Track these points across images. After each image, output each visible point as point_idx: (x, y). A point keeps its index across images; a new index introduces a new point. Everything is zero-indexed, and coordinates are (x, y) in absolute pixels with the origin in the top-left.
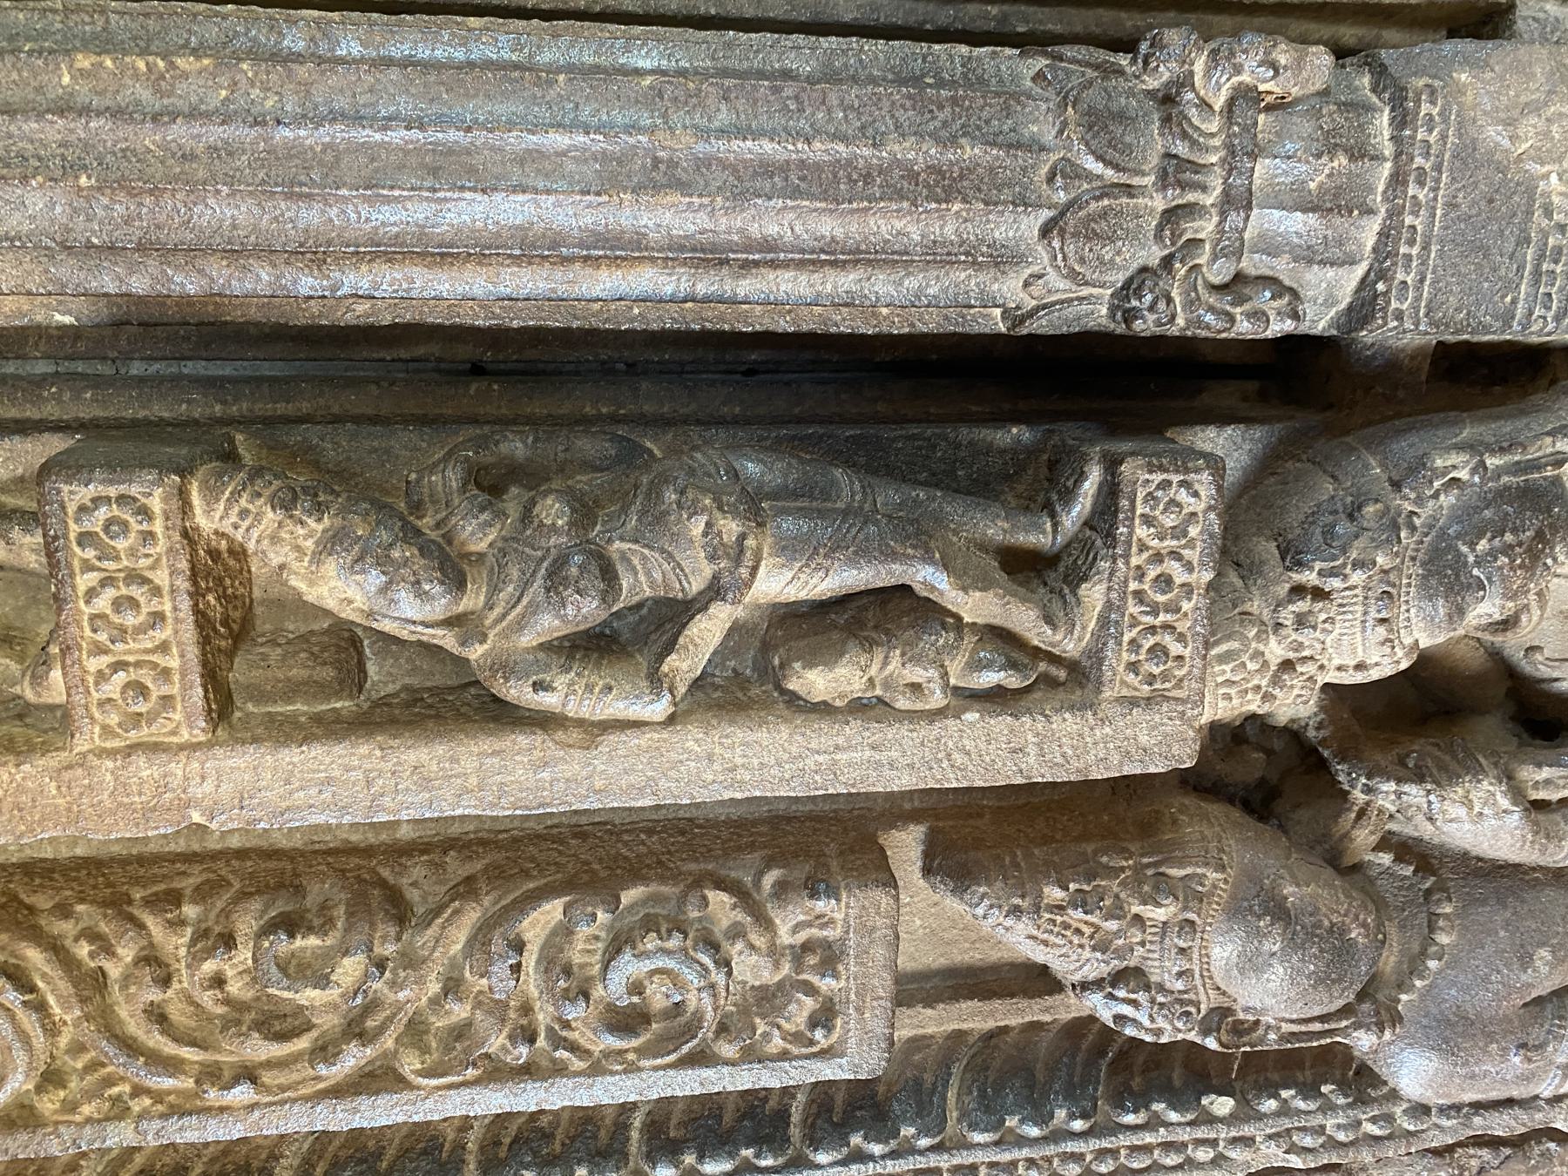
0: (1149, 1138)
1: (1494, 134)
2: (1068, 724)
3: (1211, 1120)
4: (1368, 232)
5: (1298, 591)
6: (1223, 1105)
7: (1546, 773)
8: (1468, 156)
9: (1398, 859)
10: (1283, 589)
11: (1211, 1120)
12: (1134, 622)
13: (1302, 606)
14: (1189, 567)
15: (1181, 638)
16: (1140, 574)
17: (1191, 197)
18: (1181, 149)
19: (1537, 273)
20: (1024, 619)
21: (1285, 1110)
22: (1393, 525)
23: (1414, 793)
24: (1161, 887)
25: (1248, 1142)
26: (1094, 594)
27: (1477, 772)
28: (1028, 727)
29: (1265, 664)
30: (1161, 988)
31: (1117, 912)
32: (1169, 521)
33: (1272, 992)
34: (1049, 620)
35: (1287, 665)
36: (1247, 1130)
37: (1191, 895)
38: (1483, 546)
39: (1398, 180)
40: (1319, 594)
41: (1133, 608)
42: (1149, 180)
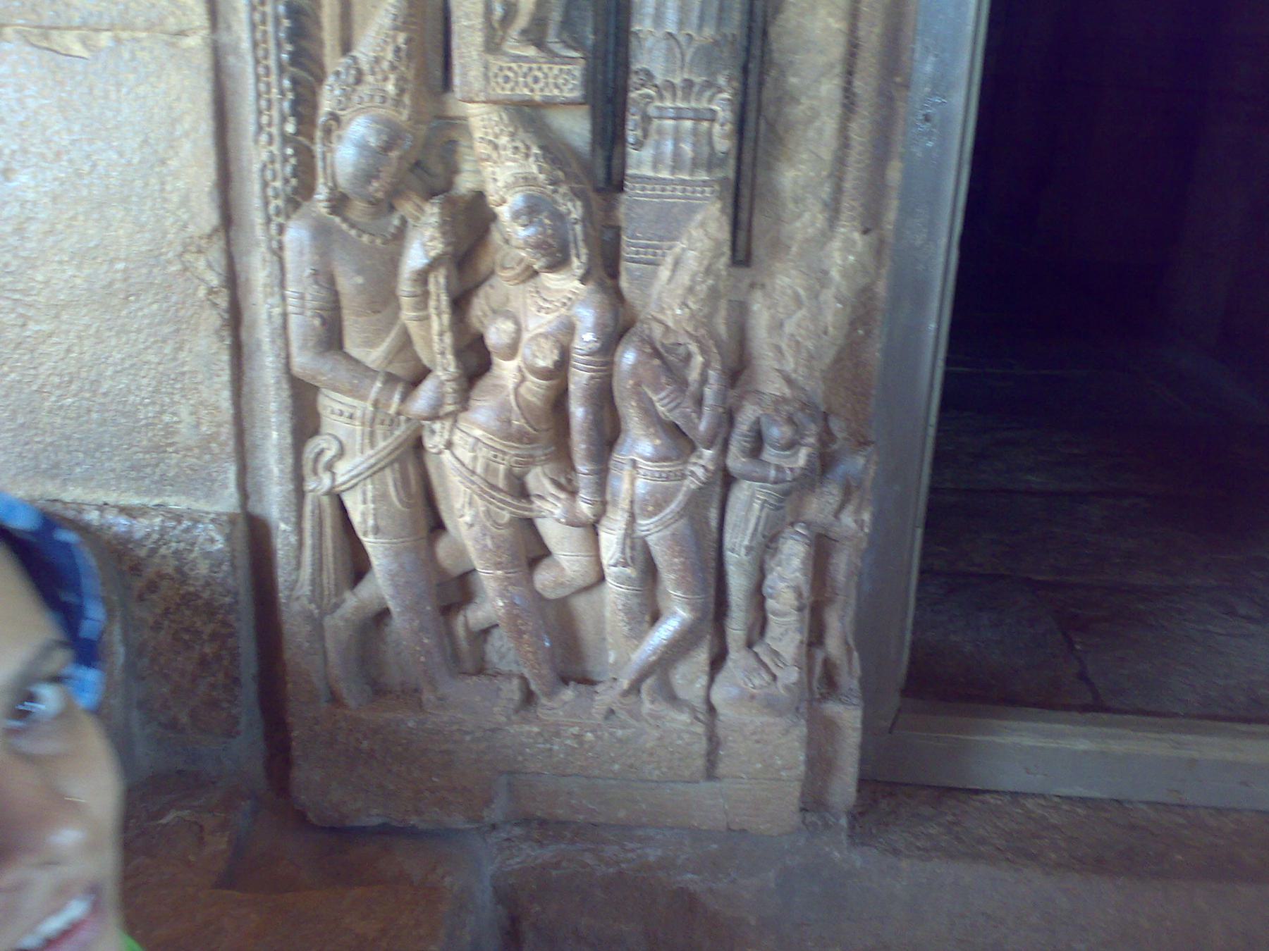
0: (275, 90)
1: (699, 217)
2: (478, 38)
3: (284, 120)
4: (665, 174)
5: (528, 148)
6: (290, 128)
7: (442, 280)
8: (690, 210)
9: (397, 227)
10: (528, 143)
11: (284, 120)
12: (520, 67)
13: (523, 150)
14: (542, 90)
15: (512, 89)
16: (540, 69)
17: (679, 93)
18: (696, 89)
19: (647, 246)
20: (522, 21)
21: (285, 159)
22: (554, 182)
23: (434, 220)
24: (401, 91)
25: (270, 142)
26: (531, 52)
27: (447, 244)
28: (478, 22)
29: (497, 136)
30: (354, 90)
31: (393, 68)
32: (561, 81)
33: (345, 155)
34: (524, 32)
35: (496, 147)
36: (277, 139)
37: (398, 102)
38: (547, 221)
39: (683, 182)
40: (527, 156)
41: (525, 69)
42: (686, 76)
